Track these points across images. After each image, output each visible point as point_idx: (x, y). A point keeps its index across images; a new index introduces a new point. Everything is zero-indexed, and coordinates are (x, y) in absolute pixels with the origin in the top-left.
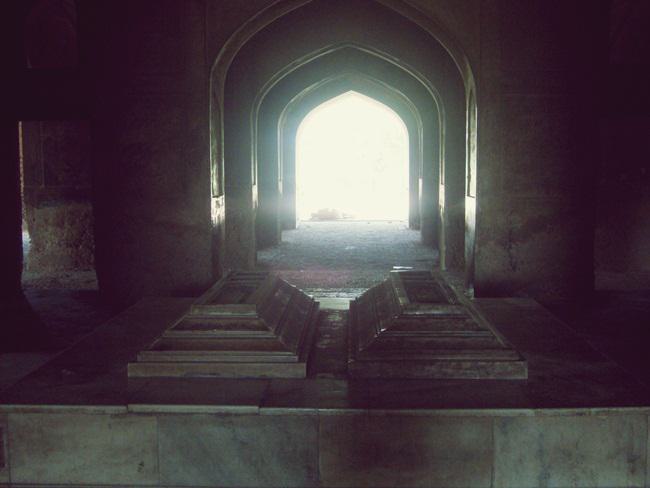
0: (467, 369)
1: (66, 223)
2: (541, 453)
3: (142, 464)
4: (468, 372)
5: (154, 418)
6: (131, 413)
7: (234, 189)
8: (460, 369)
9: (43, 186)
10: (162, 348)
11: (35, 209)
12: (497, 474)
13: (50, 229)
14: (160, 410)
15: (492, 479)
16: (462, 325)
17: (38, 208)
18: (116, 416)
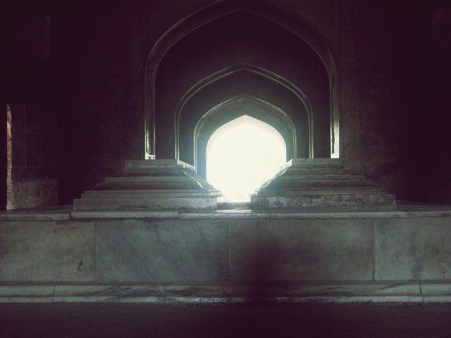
0: (347, 201)
1: (41, 194)
2: (413, 249)
3: (81, 264)
4: (348, 203)
5: (92, 224)
6: (72, 219)
7: (163, 150)
8: (341, 201)
9: (26, 167)
11: (19, 183)
12: (378, 268)
13: (30, 197)
14: (97, 216)
16: (342, 172)
17: (21, 182)
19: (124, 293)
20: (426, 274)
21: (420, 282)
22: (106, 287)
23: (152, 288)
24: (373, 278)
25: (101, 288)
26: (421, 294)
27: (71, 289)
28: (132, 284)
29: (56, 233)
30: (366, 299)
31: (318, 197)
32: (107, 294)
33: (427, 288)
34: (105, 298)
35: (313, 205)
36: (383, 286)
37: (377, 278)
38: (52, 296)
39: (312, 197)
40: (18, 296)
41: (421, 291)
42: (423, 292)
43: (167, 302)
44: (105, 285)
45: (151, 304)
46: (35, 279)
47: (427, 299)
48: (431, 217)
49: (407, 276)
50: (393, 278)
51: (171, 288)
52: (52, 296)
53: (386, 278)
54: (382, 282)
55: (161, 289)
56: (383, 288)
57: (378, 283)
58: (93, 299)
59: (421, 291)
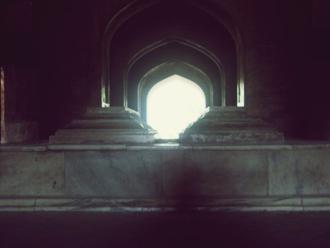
0: (249, 137)
3: (55, 183)
4: (249, 139)
5: (63, 154)
6: (48, 150)
7: (115, 100)
10: (72, 128)
12: (271, 186)
15: (268, 189)
18: (41, 152)
19: (87, 204)
20: (306, 190)
21: (302, 196)
22: (75, 200)
23: (107, 201)
24: (268, 193)
25: (69, 201)
26: (302, 205)
27: (48, 201)
28: (91, 198)
29: (36, 160)
30: (262, 209)
31: (228, 134)
32: (74, 205)
33: (306, 201)
34: (73, 208)
35: (224, 140)
36: (276, 199)
37: (270, 193)
38: (34, 206)
39: (223, 135)
40: (9, 206)
41: (302, 203)
42: (304, 204)
43: (118, 211)
44: (73, 198)
45: (106, 213)
46: (22, 194)
47: (307, 209)
48: (310, 149)
49: (292, 191)
50: (282, 193)
51: (120, 200)
52: (34, 206)
53: (276, 193)
54: (274, 196)
55: (113, 201)
56: (275, 201)
57: (271, 197)
58: (64, 209)
59: (302, 203)
